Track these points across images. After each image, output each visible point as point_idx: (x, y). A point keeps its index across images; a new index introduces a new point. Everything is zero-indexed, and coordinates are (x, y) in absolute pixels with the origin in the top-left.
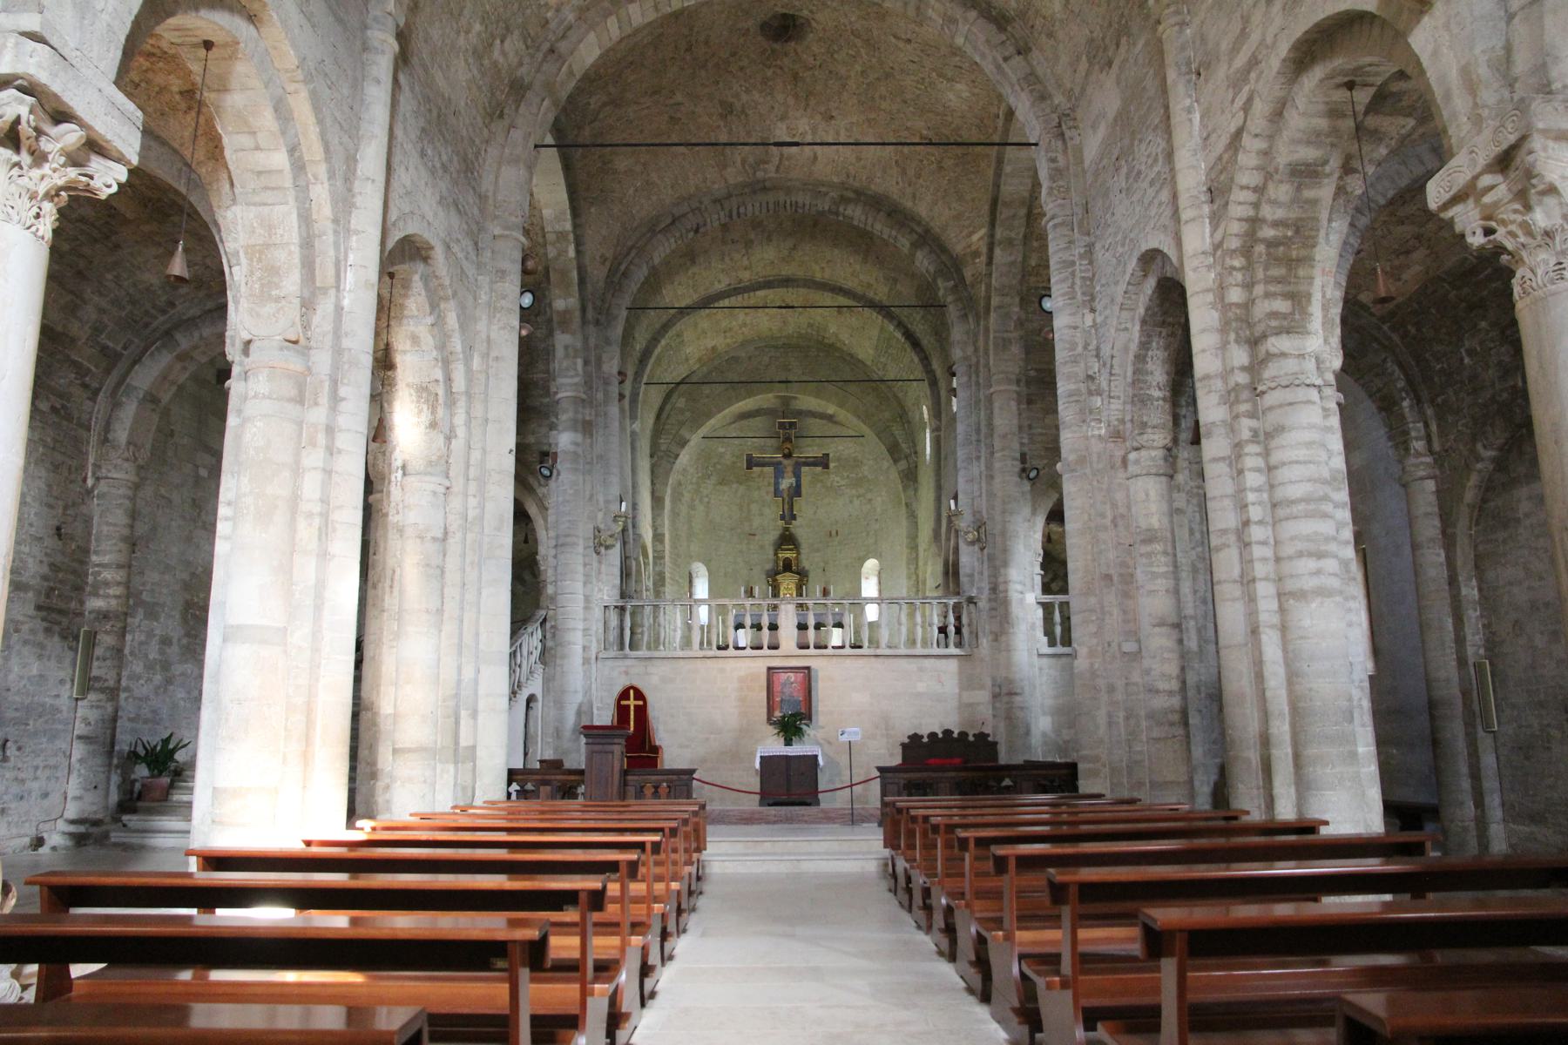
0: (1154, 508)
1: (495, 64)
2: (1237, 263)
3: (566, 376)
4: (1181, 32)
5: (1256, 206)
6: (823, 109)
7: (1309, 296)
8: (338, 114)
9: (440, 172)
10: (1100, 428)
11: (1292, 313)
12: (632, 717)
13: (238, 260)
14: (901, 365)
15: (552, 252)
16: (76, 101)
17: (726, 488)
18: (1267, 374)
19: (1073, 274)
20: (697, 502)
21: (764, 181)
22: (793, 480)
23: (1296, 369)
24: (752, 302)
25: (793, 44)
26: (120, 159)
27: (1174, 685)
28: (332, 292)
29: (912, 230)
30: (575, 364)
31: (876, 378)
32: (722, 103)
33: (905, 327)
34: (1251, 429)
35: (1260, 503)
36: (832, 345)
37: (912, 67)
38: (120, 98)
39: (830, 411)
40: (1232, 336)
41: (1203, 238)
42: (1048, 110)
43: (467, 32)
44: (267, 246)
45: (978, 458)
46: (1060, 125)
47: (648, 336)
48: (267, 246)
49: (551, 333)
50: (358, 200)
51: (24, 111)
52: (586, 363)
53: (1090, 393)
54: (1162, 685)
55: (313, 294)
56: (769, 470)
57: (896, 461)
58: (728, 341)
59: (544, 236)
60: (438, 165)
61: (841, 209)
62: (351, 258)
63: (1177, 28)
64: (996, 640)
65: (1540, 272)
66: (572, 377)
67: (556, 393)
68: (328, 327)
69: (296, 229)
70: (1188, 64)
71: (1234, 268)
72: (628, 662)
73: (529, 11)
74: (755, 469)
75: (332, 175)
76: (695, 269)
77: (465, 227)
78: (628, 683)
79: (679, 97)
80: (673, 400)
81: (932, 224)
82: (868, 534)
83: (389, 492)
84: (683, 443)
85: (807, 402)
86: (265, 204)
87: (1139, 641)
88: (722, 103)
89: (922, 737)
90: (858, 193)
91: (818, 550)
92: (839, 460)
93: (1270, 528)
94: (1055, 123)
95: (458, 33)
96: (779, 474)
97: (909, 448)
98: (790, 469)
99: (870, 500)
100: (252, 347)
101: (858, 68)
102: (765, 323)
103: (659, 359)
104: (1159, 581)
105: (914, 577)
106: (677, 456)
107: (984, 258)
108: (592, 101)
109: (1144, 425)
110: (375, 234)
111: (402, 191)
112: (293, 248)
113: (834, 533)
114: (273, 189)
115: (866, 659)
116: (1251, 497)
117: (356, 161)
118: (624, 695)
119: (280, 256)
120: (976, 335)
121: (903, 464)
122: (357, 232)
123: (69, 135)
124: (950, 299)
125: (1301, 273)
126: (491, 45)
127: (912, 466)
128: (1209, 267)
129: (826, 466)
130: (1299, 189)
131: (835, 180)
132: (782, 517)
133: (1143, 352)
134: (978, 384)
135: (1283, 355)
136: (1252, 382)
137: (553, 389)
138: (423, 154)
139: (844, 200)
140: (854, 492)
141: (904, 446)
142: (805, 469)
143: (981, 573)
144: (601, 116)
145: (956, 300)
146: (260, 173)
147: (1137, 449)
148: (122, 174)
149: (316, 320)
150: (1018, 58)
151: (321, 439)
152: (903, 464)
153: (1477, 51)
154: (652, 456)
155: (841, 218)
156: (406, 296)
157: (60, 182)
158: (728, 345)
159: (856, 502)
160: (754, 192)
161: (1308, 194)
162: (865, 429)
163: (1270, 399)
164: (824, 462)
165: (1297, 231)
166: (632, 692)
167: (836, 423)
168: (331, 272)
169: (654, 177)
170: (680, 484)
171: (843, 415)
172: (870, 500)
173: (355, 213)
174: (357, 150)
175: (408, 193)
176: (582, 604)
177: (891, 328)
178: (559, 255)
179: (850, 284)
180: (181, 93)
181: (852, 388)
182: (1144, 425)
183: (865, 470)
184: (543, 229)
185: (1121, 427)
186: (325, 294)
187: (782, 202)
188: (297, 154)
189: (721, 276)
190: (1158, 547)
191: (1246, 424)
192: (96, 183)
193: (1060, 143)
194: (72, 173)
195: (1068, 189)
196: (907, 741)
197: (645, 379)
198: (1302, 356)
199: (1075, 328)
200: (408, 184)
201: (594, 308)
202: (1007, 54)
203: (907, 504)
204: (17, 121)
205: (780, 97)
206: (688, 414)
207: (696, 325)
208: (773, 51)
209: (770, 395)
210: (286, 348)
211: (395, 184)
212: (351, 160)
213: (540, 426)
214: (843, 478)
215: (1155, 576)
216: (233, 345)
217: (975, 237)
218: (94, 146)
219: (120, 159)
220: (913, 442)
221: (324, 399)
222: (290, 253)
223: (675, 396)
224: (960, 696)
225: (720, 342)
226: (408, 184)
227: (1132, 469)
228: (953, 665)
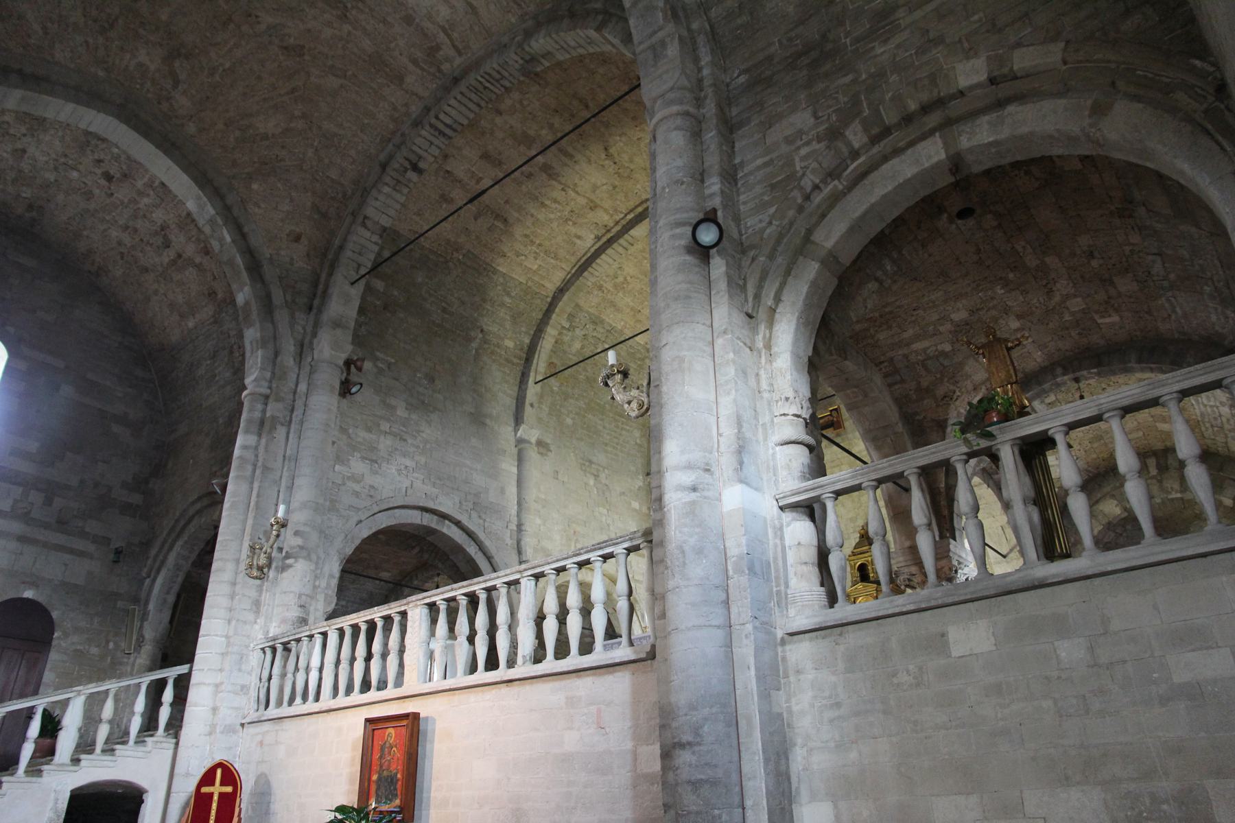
12: (213, 813)
78: (217, 759)
118: (208, 778)
139: (528, 34)
166: (219, 772)
224: (635, 755)
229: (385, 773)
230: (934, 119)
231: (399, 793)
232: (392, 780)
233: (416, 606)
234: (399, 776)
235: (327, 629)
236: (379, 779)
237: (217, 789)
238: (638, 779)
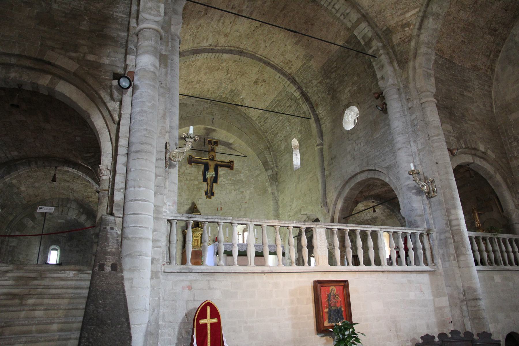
3: (150, 14)
12: (209, 337)
22: (213, 174)
30: (159, 7)
39: (231, 141)
57: (267, 170)
66: (155, 16)
72: (192, 277)
82: (240, 210)
85: (221, 135)
89: (433, 337)
96: (206, 168)
97: (273, 164)
113: (219, 209)
115: (376, 274)
118: (202, 314)
121: (270, 172)
127: (275, 173)
132: (206, 194)
140: (233, 187)
152: (270, 172)
164: (230, 166)
166: (208, 308)
167: (231, 148)
172: (242, 192)
183: (242, 176)
196: (421, 341)
209: (203, 126)
213: (116, 52)
214: (227, 180)
217: (408, 15)
224: (434, 300)
228: (426, 278)
229: (333, 308)
230: (473, 152)
231: (344, 317)
232: (338, 311)
233: (322, 228)
234: (342, 309)
235: (249, 223)
236: (330, 311)
237: (208, 321)
238: (438, 310)
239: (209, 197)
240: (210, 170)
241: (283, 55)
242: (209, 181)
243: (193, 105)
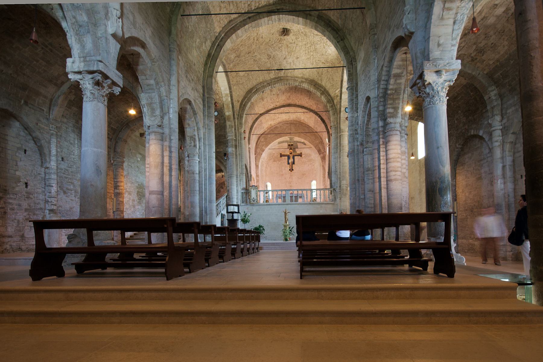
0: (369, 162)
1: (204, 50)
2: (382, 100)
4: (374, 36)
5: (387, 85)
6: (295, 55)
7: (398, 108)
8: (165, 69)
9: (191, 81)
10: (358, 143)
11: (394, 112)
13: (145, 106)
14: (321, 128)
15: (224, 99)
16: (109, 74)
17: (275, 163)
18: (387, 128)
19: (353, 103)
20: (268, 167)
21: (281, 77)
22: (293, 160)
23: (393, 126)
24: (278, 112)
25: (286, 36)
26: (119, 86)
27: (373, 206)
28: (168, 114)
29: (321, 90)
30: (232, 130)
31: (314, 131)
32: (268, 55)
33: (321, 117)
34: (383, 142)
35: (383, 159)
36: (302, 123)
37: (319, 42)
38: (117, 72)
39: (302, 141)
40: (380, 119)
41: (375, 94)
42: (349, 57)
43: (195, 42)
44: (151, 103)
45: (337, 152)
46: (352, 61)
47: (252, 122)
48: (151, 103)
49: (225, 122)
50: (172, 91)
51: (100, 78)
52: (235, 129)
53: (356, 134)
54: (369, 206)
55: (163, 115)
56: (287, 157)
57: (320, 154)
58: (275, 122)
59: (222, 95)
60: (191, 80)
61: (302, 85)
62: (171, 105)
63: (373, 36)
64: (340, 199)
65: (426, 103)
67: (227, 138)
68: (167, 123)
69: (158, 99)
70: (375, 46)
71: (381, 101)
73: (211, 34)
74: (283, 157)
75: (165, 85)
76: (264, 103)
77: (199, 95)
79: (256, 54)
80: (260, 139)
81: (326, 88)
83: (185, 163)
84: (263, 151)
85: (297, 139)
86: (150, 93)
87: (365, 195)
88: (268, 55)
90: (306, 79)
91: (300, 179)
92: (305, 154)
93: (385, 165)
94: (350, 60)
95: (193, 42)
96: (289, 158)
98: (291, 157)
99: (313, 165)
100: (150, 127)
101: (304, 43)
102: (284, 117)
103: (256, 128)
104: (370, 181)
105: (324, 185)
106: (262, 154)
107: (339, 97)
108: (232, 56)
109: (368, 142)
110: (176, 99)
111: (182, 87)
112: (157, 104)
114: (151, 89)
116: (381, 158)
117: (170, 81)
119: (155, 105)
120: (337, 119)
121: (322, 155)
122: (172, 99)
123: (109, 82)
124: (330, 109)
125: (397, 102)
126: (202, 44)
128: (376, 101)
129: (301, 156)
130: (396, 80)
131: (300, 76)
132: (290, 170)
133: (368, 123)
134: (337, 132)
135: (391, 123)
136: (384, 130)
137: (227, 137)
138: (187, 77)
139: (302, 82)
141: (322, 150)
142: (295, 157)
143: (337, 182)
144: (235, 61)
145: (332, 109)
146: (148, 85)
147: (366, 148)
148: (120, 90)
149: (164, 121)
150: (341, 42)
151: (168, 149)
152: (322, 155)
153: (418, 50)
154: (255, 154)
155: (302, 87)
156: (186, 114)
157: (108, 92)
158: (274, 123)
159: (310, 166)
160: (278, 80)
161: (398, 81)
162: (312, 146)
163: (387, 134)
164: (300, 155)
165: (396, 91)
168: (167, 109)
169: (251, 77)
170: (263, 161)
171: (306, 142)
172: (313, 165)
173: (171, 94)
174: (170, 78)
175: (184, 88)
176: (236, 192)
177: (317, 117)
178: (226, 100)
179: (306, 105)
180: (127, 65)
181: (308, 134)
182: (368, 142)
184: (221, 93)
185: (362, 143)
186: (166, 114)
187: (285, 83)
188: (156, 80)
189: (271, 104)
190: (370, 172)
191: (381, 140)
192: (115, 92)
193: (351, 66)
194: (110, 90)
195: (353, 80)
197: (252, 134)
198: (395, 123)
199: (353, 117)
200: (184, 85)
201: (237, 115)
202: (338, 40)
203: (323, 166)
204: (99, 80)
205: (284, 52)
206: (264, 143)
207: (265, 118)
208: (281, 39)
210: (158, 128)
211: (180, 86)
212: (169, 81)
215: (369, 179)
216: (145, 127)
217: (337, 91)
218: (114, 84)
219: (119, 86)
220: (325, 149)
221: (168, 140)
222: (157, 105)
223: (261, 138)
225: (272, 123)
226: (184, 85)
227: (365, 153)
239: (291, 171)
240: (290, 159)
241: (308, 103)
242: (290, 164)
243: (281, 127)
